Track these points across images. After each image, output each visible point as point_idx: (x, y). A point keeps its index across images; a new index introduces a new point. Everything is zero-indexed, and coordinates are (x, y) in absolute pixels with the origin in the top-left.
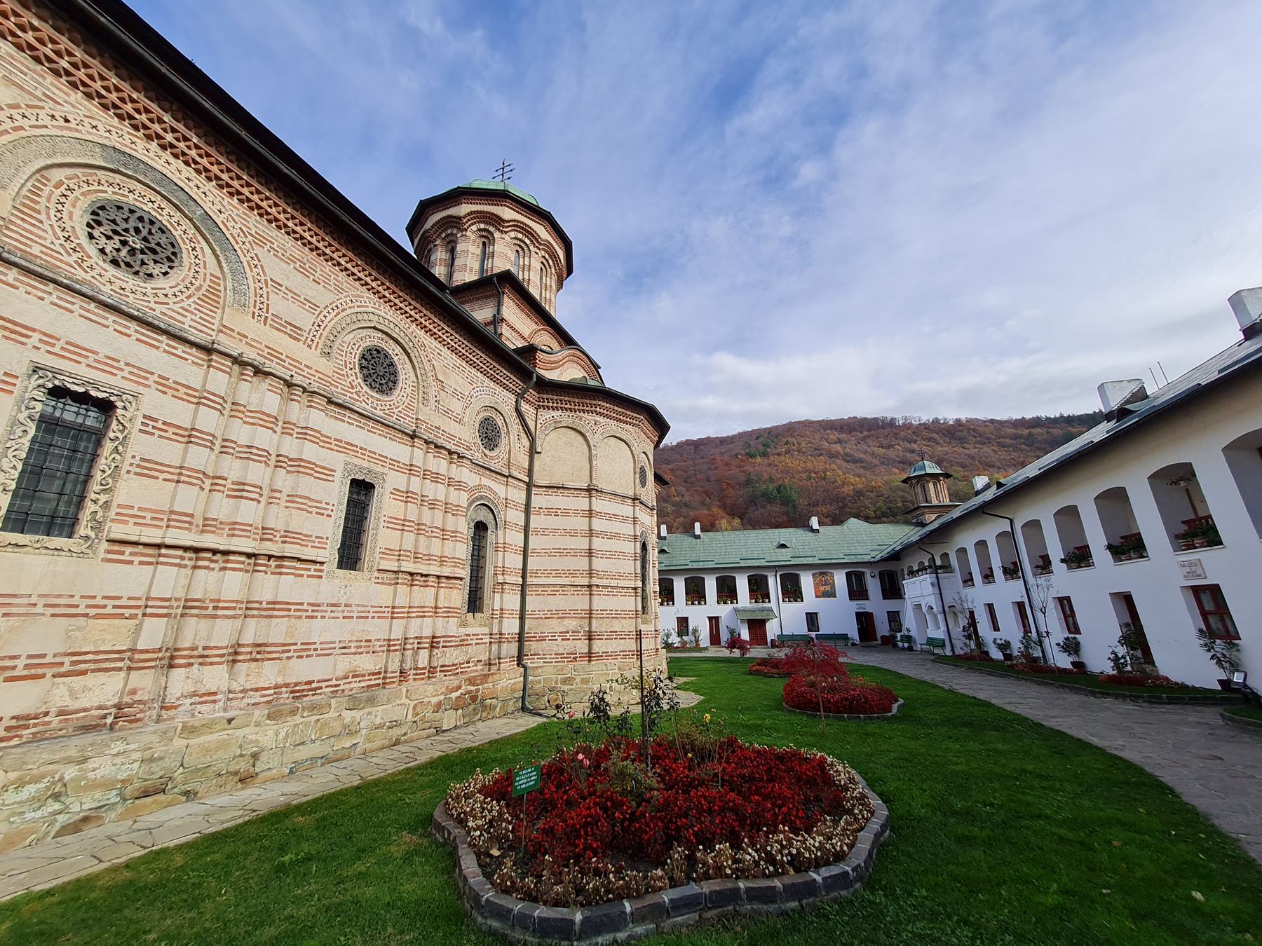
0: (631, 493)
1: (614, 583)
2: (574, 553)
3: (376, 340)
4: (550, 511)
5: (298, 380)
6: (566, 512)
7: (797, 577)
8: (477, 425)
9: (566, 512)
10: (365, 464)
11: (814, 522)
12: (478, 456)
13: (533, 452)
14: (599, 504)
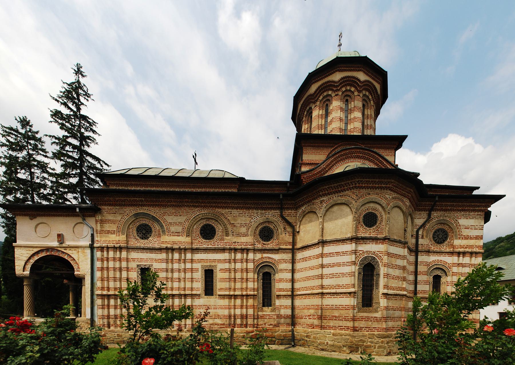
3: (204, 222)
4: (304, 259)
5: (182, 247)
8: (258, 232)
10: (208, 264)
12: (259, 246)
14: (328, 249)
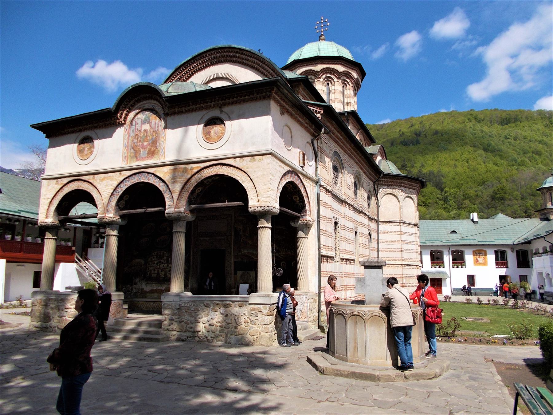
0: (413, 222)
1: (409, 263)
2: (395, 250)
6: (391, 232)
7: (462, 252)
9: (391, 232)
11: (475, 216)
13: (378, 206)
